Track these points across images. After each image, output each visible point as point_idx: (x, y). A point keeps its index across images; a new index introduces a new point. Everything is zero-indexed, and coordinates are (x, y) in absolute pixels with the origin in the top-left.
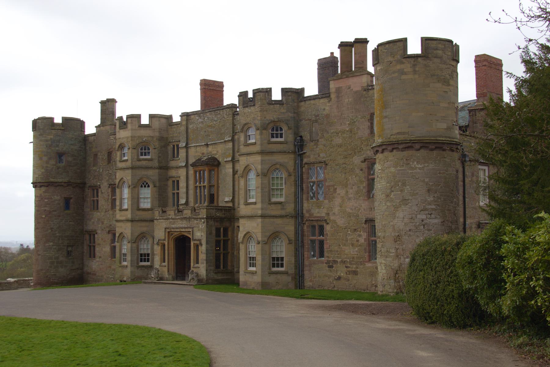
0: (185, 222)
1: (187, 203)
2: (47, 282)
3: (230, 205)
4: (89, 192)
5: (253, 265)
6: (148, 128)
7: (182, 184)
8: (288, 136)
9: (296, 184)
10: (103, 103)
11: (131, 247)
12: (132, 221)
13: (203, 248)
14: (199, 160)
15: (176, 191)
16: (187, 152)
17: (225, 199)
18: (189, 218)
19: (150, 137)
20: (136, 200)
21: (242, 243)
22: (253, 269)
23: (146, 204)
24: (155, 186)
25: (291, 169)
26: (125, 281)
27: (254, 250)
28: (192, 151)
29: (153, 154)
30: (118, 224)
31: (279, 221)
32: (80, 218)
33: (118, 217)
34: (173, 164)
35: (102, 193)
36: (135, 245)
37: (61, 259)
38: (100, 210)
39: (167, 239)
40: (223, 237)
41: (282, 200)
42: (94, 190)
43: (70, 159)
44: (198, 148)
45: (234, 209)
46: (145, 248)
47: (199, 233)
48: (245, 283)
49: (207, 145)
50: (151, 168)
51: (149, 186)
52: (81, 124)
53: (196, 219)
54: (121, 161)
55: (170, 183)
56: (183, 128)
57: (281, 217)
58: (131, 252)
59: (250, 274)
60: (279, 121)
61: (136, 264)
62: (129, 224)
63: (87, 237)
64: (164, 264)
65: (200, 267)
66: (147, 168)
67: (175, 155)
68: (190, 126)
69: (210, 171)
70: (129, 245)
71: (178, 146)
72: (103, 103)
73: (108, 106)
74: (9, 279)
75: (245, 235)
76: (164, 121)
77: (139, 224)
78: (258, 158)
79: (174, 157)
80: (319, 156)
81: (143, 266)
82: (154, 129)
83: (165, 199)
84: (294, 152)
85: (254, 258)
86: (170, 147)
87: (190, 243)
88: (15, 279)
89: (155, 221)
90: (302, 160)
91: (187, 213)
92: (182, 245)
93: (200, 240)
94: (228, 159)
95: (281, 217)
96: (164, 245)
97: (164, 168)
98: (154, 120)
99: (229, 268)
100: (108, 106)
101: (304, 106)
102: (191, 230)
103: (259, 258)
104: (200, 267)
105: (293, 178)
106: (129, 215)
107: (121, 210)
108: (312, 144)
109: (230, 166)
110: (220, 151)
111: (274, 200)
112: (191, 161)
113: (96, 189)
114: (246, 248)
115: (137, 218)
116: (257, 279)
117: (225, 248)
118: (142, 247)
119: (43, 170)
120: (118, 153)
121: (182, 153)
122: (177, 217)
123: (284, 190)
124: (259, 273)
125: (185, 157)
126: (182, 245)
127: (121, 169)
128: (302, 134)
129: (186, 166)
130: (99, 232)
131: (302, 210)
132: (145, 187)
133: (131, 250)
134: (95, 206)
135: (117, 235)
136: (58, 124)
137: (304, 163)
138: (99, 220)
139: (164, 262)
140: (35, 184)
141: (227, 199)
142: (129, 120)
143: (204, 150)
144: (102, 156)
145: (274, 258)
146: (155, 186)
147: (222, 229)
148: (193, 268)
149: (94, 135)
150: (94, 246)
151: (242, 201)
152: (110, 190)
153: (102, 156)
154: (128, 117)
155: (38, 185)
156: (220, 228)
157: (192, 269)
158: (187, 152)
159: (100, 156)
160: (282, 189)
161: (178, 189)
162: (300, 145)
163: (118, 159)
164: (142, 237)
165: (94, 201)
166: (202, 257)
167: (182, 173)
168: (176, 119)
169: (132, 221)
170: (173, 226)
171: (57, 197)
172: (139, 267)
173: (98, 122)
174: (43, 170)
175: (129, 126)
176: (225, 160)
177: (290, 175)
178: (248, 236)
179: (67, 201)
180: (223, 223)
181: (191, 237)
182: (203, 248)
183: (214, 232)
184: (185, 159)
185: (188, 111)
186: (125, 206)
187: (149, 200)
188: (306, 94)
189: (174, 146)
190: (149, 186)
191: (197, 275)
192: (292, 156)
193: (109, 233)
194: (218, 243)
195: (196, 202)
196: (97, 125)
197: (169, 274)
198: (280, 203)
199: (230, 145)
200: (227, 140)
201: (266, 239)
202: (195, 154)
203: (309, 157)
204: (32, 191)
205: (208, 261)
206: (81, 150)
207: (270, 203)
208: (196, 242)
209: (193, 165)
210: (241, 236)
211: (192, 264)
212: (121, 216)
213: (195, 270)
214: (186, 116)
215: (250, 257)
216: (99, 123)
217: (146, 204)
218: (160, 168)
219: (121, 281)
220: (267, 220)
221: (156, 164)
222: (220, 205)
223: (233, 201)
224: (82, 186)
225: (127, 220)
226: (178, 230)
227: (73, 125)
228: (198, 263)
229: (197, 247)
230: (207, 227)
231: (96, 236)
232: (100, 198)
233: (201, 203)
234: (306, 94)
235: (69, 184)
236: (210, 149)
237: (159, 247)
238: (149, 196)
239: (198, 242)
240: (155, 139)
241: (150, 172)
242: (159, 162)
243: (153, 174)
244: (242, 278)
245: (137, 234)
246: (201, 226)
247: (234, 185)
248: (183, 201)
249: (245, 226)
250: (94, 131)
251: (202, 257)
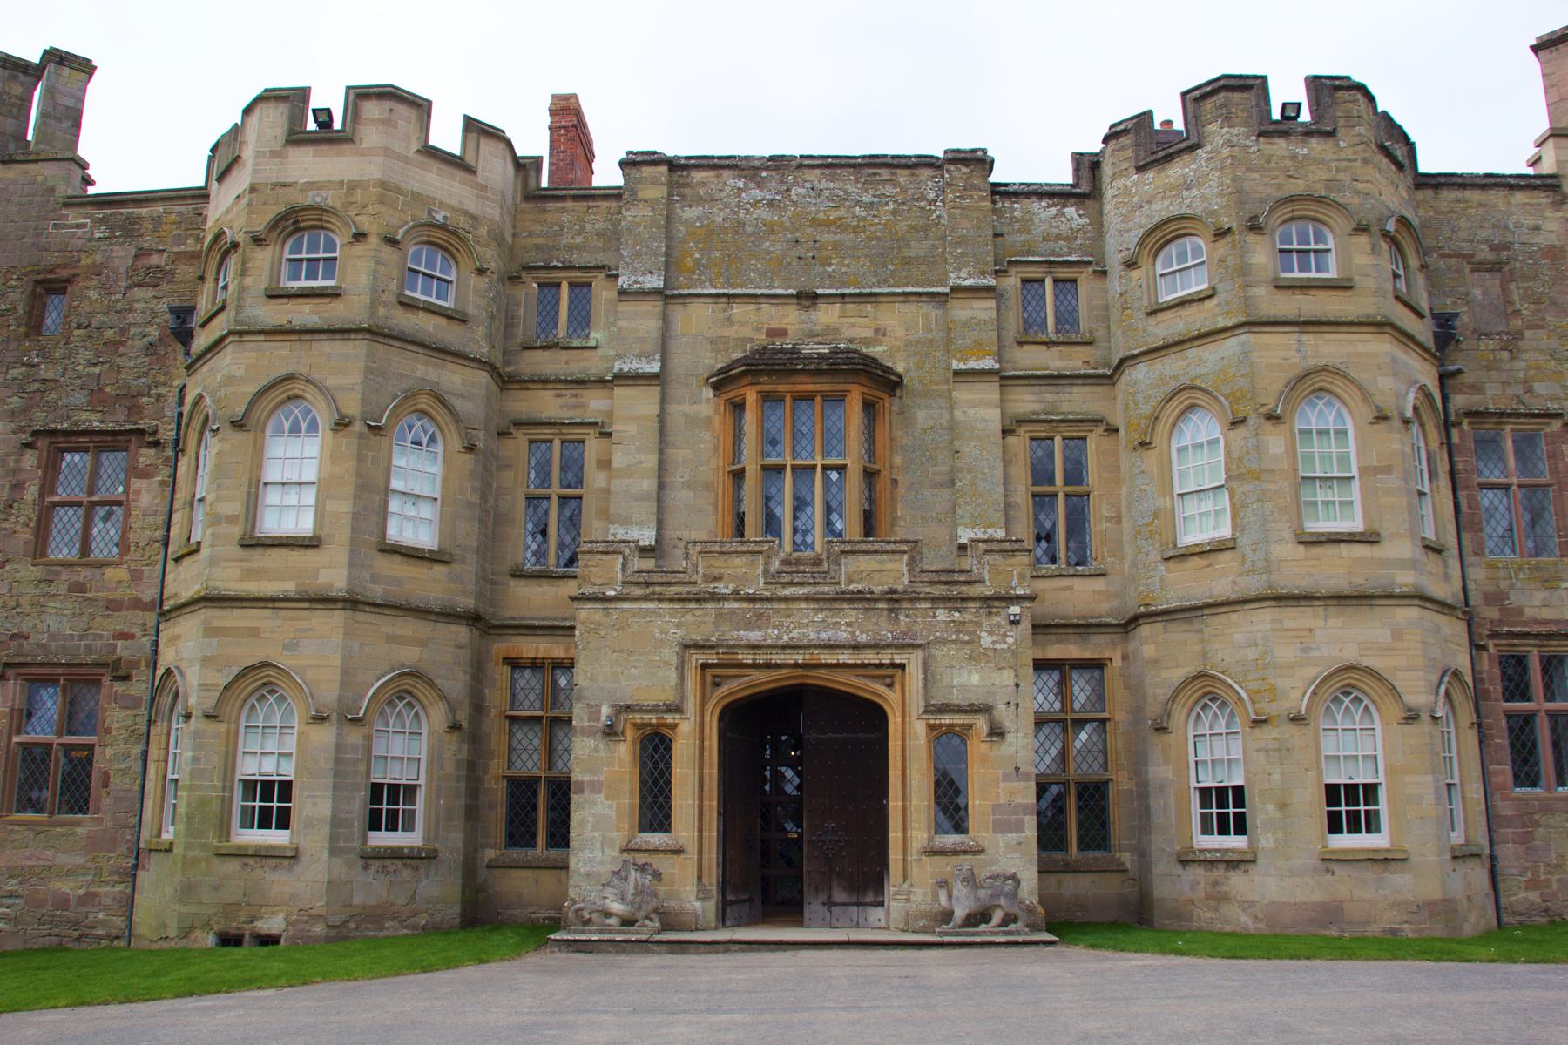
6: (460, 174)
11: (339, 747)
12: (352, 603)
19: (465, 213)
23: (414, 527)
26: (269, 940)
36: (355, 736)
58: (337, 774)
61: (357, 844)
62: (331, 622)
70: (324, 736)
81: (396, 854)
82: (484, 188)
115: (377, 592)
133: (338, 761)
169: (352, 603)
219: (229, 940)
240: (483, 231)
241: (453, 378)
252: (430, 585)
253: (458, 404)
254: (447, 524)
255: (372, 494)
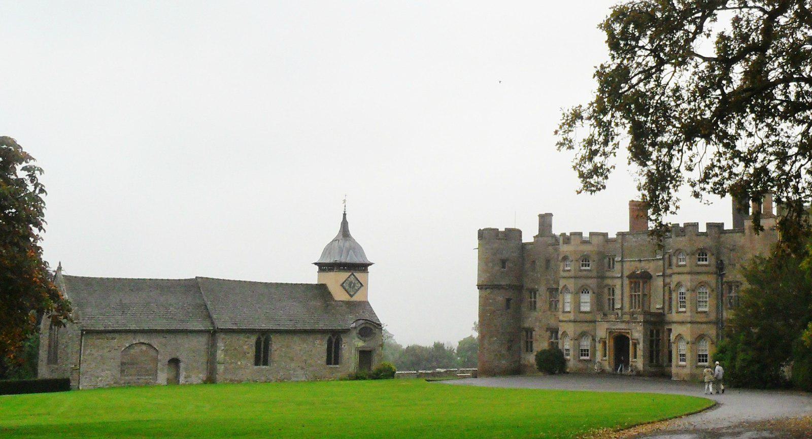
0: (624, 324)
1: (621, 308)
2: (489, 372)
3: (661, 311)
4: (526, 295)
5: (684, 360)
7: (618, 292)
8: (710, 260)
9: (717, 299)
10: (542, 217)
12: (575, 321)
13: (640, 346)
14: (634, 272)
15: (612, 297)
16: (622, 266)
17: (656, 306)
18: (628, 322)
20: (577, 305)
21: (674, 343)
22: (683, 363)
23: (586, 308)
24: (594, 293)
25: (714, 286)
27: (683, 347)
28: (626, 265)
29: (592, 266)
30: (561, 324)
31: (704, 326)
32: (518, 317)
33: (561, 318)
34: (608, 274)
35: (540, 295)
36: (576, 342)
37: (503, 352)
38: (537, 310)
39: (607, 337)
40: (656, 336)
41: (706, 309)
42: (531, 293)
43: (511, 265)
44: (633, 263)
45: (664, 315)
46: (586, 344)
47: (637, 333)
48: (677, 375)
49: (640, 261)
50: (591, 278)
51: (588, 293)
52: (519, 233)
53: (635, 322)
54: (564, 271)
55: (606, 290)
56: (618, 245)
57: (706, 323)
59: (681, 367)
60: (705, 249)
62: (571, 325)
63: (524, 333)
64: (605, 358)
65: (639, 362)
66: (587, 278)
67: (611, 267)
68: (626, 244)
69: (644, 283)
70: (572, 342)
71: (613, 260)
72: (542, 217)
73: (545, 221)
74: (438, 370)
75: (677, 336)
76: (601, 237)
77: (581, 325)
78: (688, 277)
79: (610, 268)
80: (736, 277)
81: (585, 360)
83: (603, 306)
84: (716, 273)
85: (684, 355)
86: (606, 260)
87: (629, 341)
88: (445, 370)
89: (597, 323)
90: (722, 280)
91: (627, 318)
92: (621, 344)
93: (637, 340)
94: (659, 274)
95: (706, 323)
96: (605, 343)
97: (602, 277)
98: (594, 237)
99: (660, 363)
100: (545, 221)
101: (724, 237)
102: (630, 331)
103: (688, 356)
104: (639, 362)
105: (715, 293)
106: (571, 316)
107: (564, 312)
108: (731, 267)
109: (661, 279)
110: (650, 267)
111: (700, 309)
112: (626, 273)
113: (533, 292)
114: (677, 347)
116: (687, 371)
117: (657, 345)
118: (582, 343)
119: (488, 275)
120: (562, 264)
121: (618, 266)
122: (617, 320)
123: (708, 303)
124: (689, 366)
125: (620, 269)
126: (621, 344)
127: (564, 278)
128: (722, 258)
129: (622, 277)
130: (536, 329)
131: (722, 317)
132: (585, 293)
134: (533, 306)
135: (560, 333)
136: (502, 232)
137: (724, 281)
138: (536, 319)
139: (605, 356)
140: (480, 287)
141: (658, 306)
142: (572, 237)
143: (638, 264)
144: (540, 263)
145: (699, 355)
146: (594, 293)
147: (655, 331)
148: (632, 362)
149: (530, 244)
150: (532, 342)
151: (674, 310)
152: (548, 293)
153: (540, 263)
154: (571, 234)
155: (484, 287)
156: (653, 330)
157: (631, 363)
158: (622, 266)
159: (538, 263)
160: (706, 302)
161: (613, 295)
162: (720, 268)
163: (561, 268)
164: (583, 334)
165: (531, 302)
166: (640, 353)
167: (618, 283)
168: (612, 235)
169: (575, 321)
170: (614, 327)
171: (500, 298)
172: (580, 361)
173: (537, 233)
174: (488, 275)
175: (572, 242)
176: (657, 274)
177: (713, 291)
178: (680, 337)
179: (508, 300)
180: (657, 326)
181: (630, 337)
182: (640, 346)
183: (649, 333)
184: (620, 271)
185: (623, 231)
186: (568, 309)
187: (589, 304)
188: (725, 229)
189: (610, 259)
190: (588, 293)
191: (636, 367)
192: (715, 276)
193: (547, 331)
194: (652, 342)
195: (631, 307)
196: (535, 235)
197: (610, 367)
198: (705, 312)
199: (661, 262)
200: (658, 258)
201: (694, 340)
202: (630, 267)
203: (728, 277)
204: (476, 292)
205: (644, 356)
206: (519, 257)
207: (698, 313)
208: (633, 341)
209: (629, 277)
210: (672, 337)
211: (630, 359)
212: (564, 317)
213: (634, 364)
214: (621, 235)
215: (681, 354)
216: (537, 233)
217: (586, 308)
218: (598, 277)
220: (695, 326)
221: (594, 274)
222: (652, 311)
223: (663, 308)
224: (519, 288)
225: (570, 321)
226: (619, 331)
227: (513, 234)
228: (635, 357)
229: (635, 345)
230: (644, 329)
231: (534, 333)
232: (537, 300)
233: (635, 308)
234: (726, 228)
235: (511, 287)
236: (643, 264)
237: (601, 344)
238: (589, 301)
239: (636, 341)
241: (589, 282)
242: (598, 272)
243: (592, 283)
244: (674, 370)
245: (577, 333)
246: (638, 329)
247: (664, 295)
248: (618, 306)
249: (676, 330)
250: (532, 240)
251: (640, 353)
252: (589, 317)
253: (591, 286)
254: (592, 305)
255: (577, 305)
